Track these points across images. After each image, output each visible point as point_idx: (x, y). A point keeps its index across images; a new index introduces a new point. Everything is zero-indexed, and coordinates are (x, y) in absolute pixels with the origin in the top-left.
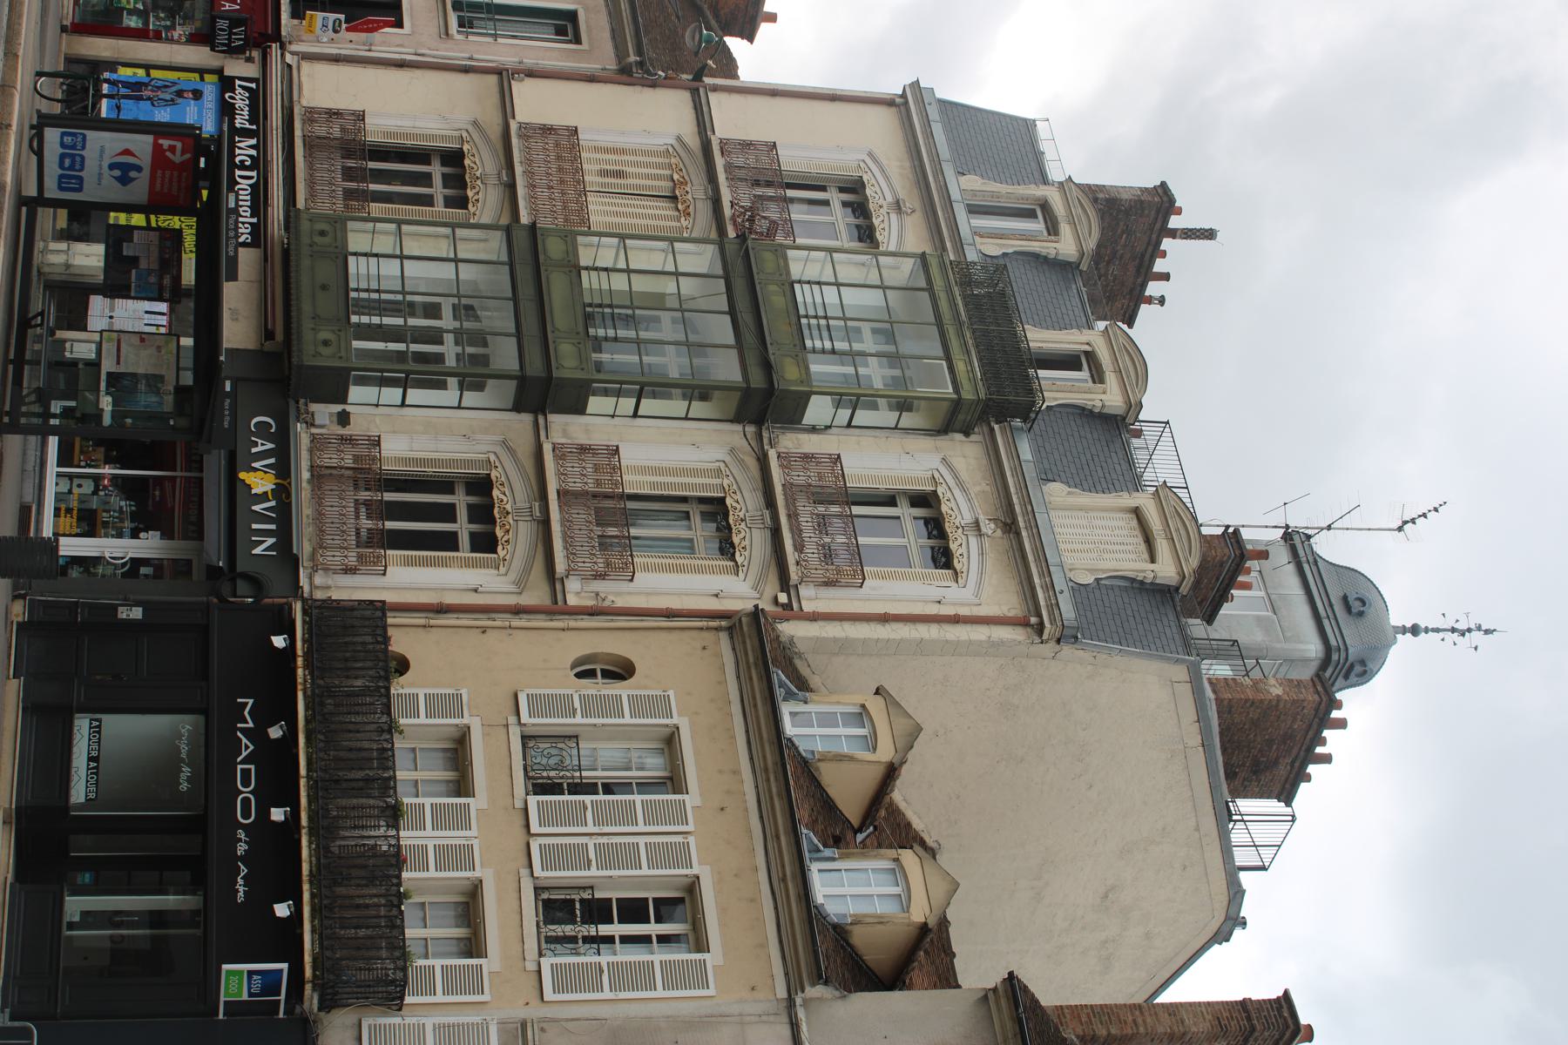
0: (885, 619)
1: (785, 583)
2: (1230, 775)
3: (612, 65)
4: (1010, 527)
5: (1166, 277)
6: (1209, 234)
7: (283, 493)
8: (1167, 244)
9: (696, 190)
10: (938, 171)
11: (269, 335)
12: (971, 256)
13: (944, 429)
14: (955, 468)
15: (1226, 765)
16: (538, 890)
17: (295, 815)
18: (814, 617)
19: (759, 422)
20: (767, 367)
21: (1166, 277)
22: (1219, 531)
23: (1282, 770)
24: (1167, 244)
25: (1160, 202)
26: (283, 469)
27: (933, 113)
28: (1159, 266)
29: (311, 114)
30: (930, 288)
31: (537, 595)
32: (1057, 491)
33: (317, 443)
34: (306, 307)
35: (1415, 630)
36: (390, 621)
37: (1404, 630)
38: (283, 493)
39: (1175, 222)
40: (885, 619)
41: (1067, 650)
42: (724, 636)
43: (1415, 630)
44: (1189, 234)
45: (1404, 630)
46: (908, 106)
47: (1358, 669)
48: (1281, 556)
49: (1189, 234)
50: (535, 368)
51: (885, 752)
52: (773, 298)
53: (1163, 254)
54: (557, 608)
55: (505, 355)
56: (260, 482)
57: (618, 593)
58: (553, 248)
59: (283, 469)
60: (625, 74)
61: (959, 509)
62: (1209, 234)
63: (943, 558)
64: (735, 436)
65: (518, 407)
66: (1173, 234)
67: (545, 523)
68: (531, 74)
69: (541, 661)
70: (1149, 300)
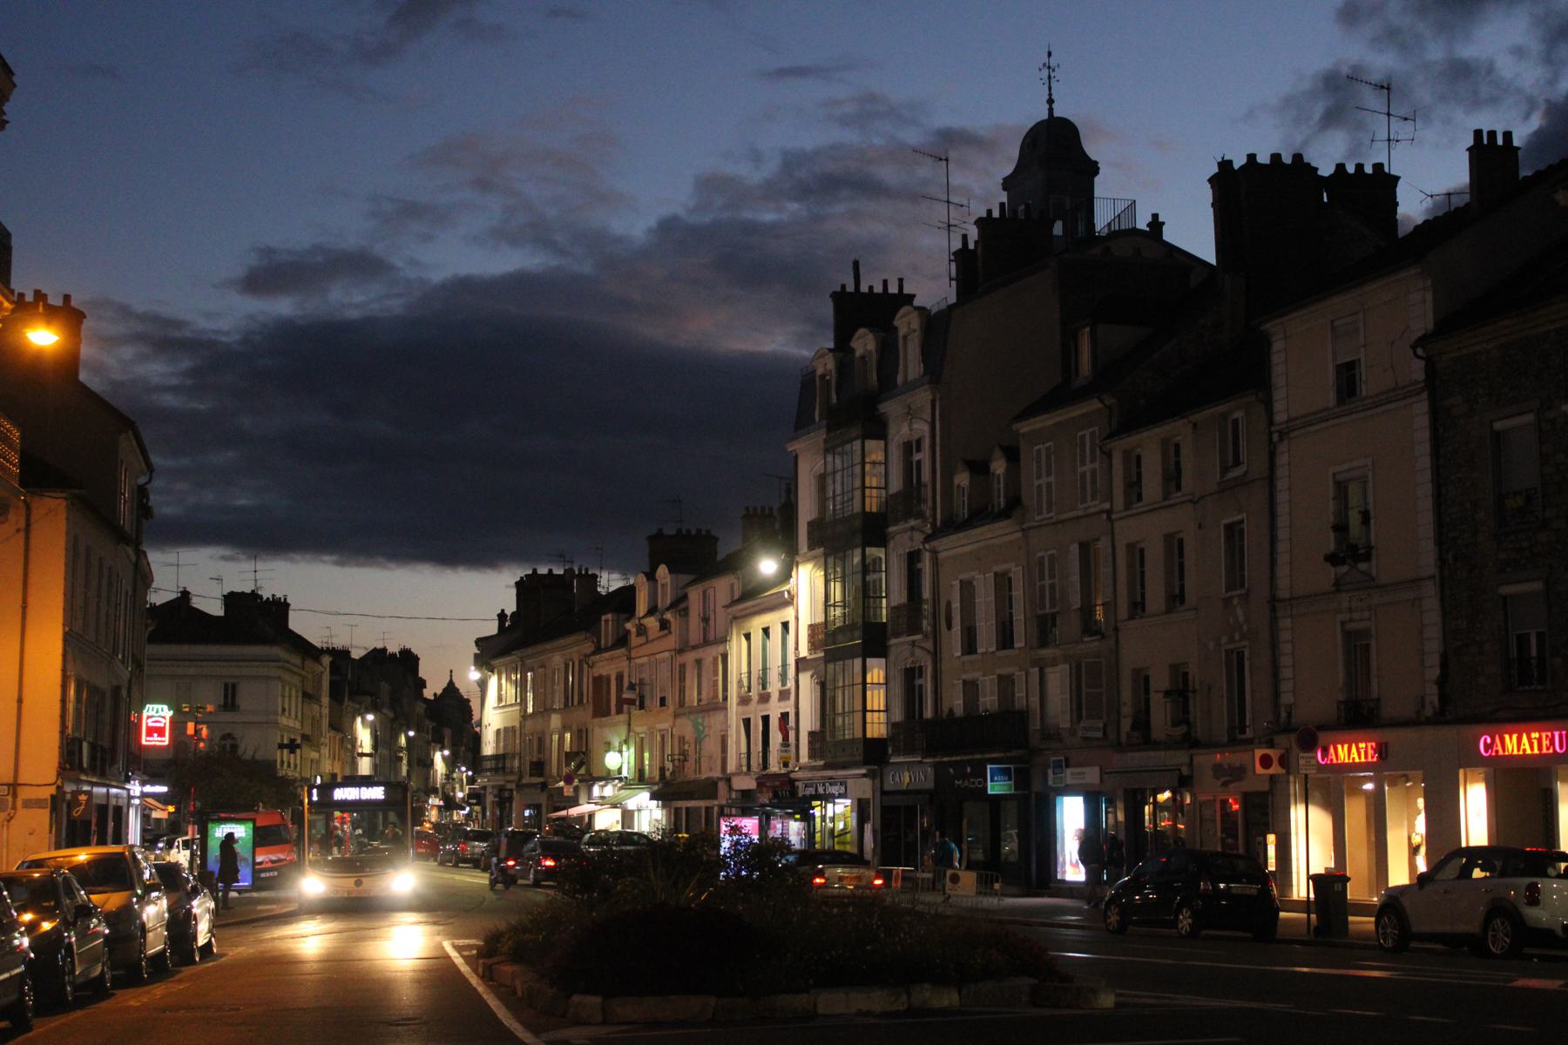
5: (885, 283)
6: (856, 265)
8: (864, 288)
17: (970, 762)
21: (885, 283)
22: (953, 266)
25: (840, 298)
28: (878, 289)
33: (897, 752)
35: (1050, 101)
37: (1051, 110)
39: (850, 288)
43: (1050, 101)
45: (1051, 110)
53: (871, 288)
62: (856, 265)
68: (797, 649)
70: (901, 287)
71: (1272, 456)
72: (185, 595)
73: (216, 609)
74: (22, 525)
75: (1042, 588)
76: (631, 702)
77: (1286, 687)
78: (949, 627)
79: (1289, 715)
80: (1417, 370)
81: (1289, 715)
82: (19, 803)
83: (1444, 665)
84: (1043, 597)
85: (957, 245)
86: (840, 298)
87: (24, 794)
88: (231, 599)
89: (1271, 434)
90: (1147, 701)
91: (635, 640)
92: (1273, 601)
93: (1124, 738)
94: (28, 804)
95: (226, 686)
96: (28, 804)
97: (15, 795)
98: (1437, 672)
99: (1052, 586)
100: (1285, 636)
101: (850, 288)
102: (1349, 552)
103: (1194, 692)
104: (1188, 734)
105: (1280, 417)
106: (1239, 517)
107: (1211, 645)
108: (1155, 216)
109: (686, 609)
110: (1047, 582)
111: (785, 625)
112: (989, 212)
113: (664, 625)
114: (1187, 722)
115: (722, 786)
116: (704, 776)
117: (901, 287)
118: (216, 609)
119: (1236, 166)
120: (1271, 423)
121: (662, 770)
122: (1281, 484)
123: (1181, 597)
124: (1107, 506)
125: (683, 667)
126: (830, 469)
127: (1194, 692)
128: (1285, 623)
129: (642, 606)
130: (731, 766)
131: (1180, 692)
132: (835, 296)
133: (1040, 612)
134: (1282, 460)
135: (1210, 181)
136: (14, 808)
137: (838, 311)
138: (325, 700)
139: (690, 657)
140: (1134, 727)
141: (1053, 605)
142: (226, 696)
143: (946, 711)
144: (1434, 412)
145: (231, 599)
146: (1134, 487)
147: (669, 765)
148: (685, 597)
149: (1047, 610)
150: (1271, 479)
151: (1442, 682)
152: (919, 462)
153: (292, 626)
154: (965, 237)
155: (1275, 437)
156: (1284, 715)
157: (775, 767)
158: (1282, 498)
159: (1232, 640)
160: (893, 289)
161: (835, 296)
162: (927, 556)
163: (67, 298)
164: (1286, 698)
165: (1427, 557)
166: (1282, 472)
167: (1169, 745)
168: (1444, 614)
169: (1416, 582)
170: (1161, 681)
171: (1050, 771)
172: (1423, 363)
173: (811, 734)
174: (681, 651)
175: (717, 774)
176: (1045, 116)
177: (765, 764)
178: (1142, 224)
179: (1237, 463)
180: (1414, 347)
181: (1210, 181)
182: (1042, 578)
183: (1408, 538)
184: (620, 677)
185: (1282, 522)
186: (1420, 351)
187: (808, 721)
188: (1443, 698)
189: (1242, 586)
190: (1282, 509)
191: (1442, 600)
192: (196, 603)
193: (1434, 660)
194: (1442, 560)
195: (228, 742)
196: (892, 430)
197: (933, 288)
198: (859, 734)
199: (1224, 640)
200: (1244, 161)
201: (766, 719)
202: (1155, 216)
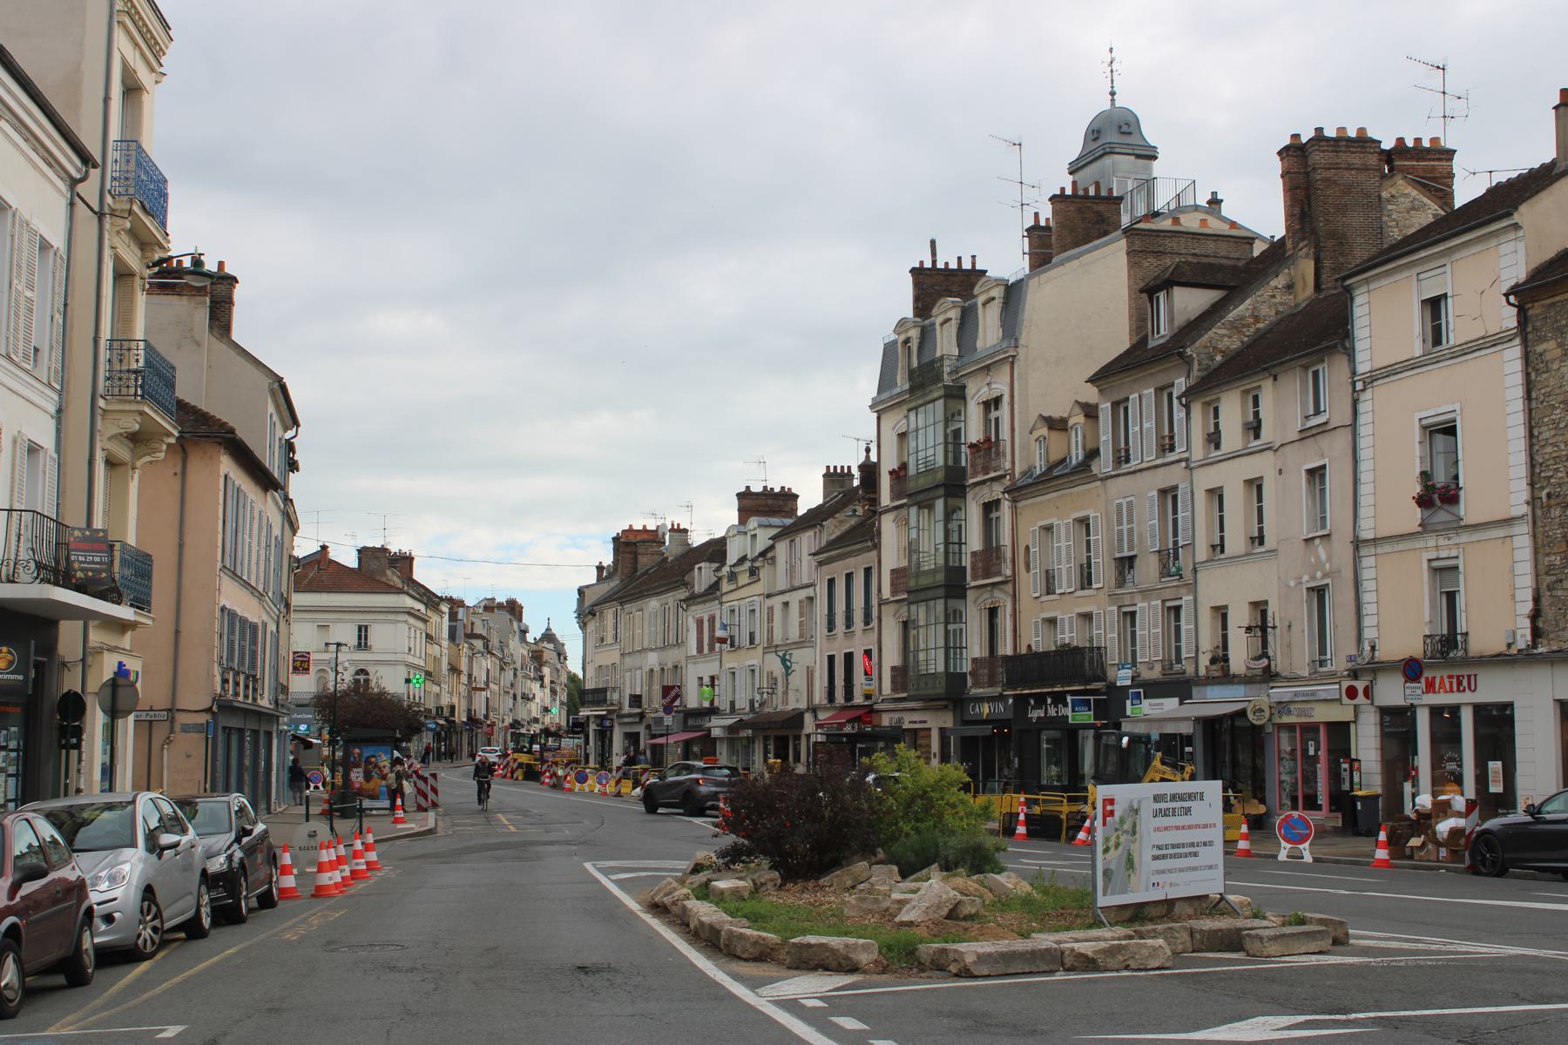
0: (1013, 430)
1: (1003, 477)
2: (1106, 233)
3: (875, 553)
4: (988, 368)
6: (933, 243)
7: (990, 699)
8: (940, 265)
9: (904, 512)
10: (892, 398)
11: (946, 707)
12: (907, 386)
13: (963, 398)
14: (978, 391)
15: (1099, 237)
16: (1083, 588)
18: (1013, 463)
19: (964, 487)
20: (937, 487)
23: (1101, 208)
24: (940, 265)
25: (918, 273)
26: (980, 700)
27: (885, 396)
28: (953, 265)
29: (894, 689)
30: (916, 408)
31: (1009, 588)
32: (979, 344)
33: (976, 684)
34: (931, 692)
35: (1113, 94)
36: (1009, 652)
37: (1113, 100)
38: (990, 699)
39: (928, 265)
40: (1013, 430)
41: (1021, 342)
42: (1020, 505)
43: (1113, 94)
44: (934, 254)
45: (1113, 100)
46: (881, 408)
47: (1125, 128)
48: (1079, 176)
49: (934, 254)
50: (941, 592)
51: (1044, 431)
52: (923, 483)
54: (1013, 580)
55: (940, 605)
56: (986, 709)
57: (1009, 555)
58: (912, 583)
59: (980, 700)
60: (877, 546)
61: (986, 394)
62: (933, 243)
63: (997, 401)
64: (970, 496)
65: (965, 597)
66: (934, 262)
67: (994, 585)
68: (880, 590)
69: (1030, 584)
70: (974, 264)
71: (1355, 402)
72: (324, 548)
73: (351, 561)
74: (178, 469)
75: (1120, 532)
76: (722, 641)
77: (1367, 622)
78: (1028, 570)
79: (1373, 648)
80: (1508, 318)
81: (1373, 648)
82: (177, 728)
83: (1537, 600)
84: (1120, 540)
85: (1030, 222)
86: (918, 273)
87: (182, 719)
88: (363, 552)
89: (1354, 383)
90: (1225, 638)
91: (725, 587)
92: (1357, 543)
93: (1202, 672)
94: (186, 728)
95: (360, 628)
96: (186, 728)
97: (172, 721)
98: (1529, 606)
99: (1131, 531)
100: (1367, 574)
101: (928, 265)
102: (1438, 496)
103: (1274, 627)
104: (1267, 669)
105: (1362, 368)
106: (1321, 463)
107: (1292, 583)
108: (1214, 194)
109: (773, 558)
110: (1125, 527)
111: (868, 571)
112: (1063, 189)
113: (753, 572)
114: (1265, 655)
115: (808, 718)
116: (790, 708)
117: (974, 264)
118: (351, 561)
119: (1304, 140)
120: (1354, 373)
121: (752, 702)
122: (1364, 430)
123: (1260, 539)
124: (1186, 455)
125: (771, 609)
126: (913, 426)
127: (1274, 627)
128: (1367, 562)
129: (732, 556)
130: (817, 701)
131: (1261, 626)
132: (913, 271)
133: (1118, 555)
134: (1361, 408)
135: (1279, 153)
136: (172, 731)
137: (917, 285)
138: (445, 643)
139: (777, 602)
140: (1213, 661)
141: (1131, 548)
142: (360, 637)
143: (1024, 651)
144: (1527, 358)
145: (363, 552)
146: (1214, 439)
147: (758, 697)
148: (772, 547)
149: (1126, 553)
150: (1354, 426)
151: (1535, 616)
152: (997, 419)
153: (415, 577)
154: (1036, 215)
155: (1359, 386)
156: (1367, 648)
157: (858, 699)
158: (1364, 443)
159: (1313, 578)
160: (967, 265)
161: (913, 271)
162: (1006, 506)
163: (221, 264)
164: (1369, 634)
165: (1517, 499)
166: (1362, 419)
167: (1247, 680)
168: (1536, 552)
169: (1508, 521)
170: (1240, 617)
171: (1128, 702)
172: (1515, 310)
173: (893, 669)
174: (769, 596)
175: (803, 705)
176: (1107, 106)
177: (849, 694)
178: (1202, 200)
179: (1317, 412)
180: (1507, 295)
181: (1279, 153)
182: (1120, 523)
183: (1496, 476)
184: (712, 619)
185: (1365, 466)
186: (1512, 299)
187: (891, 656)
188: (1536, 633)
189: (1323, 526)
190: (1365, 454)
191: (1534, 536)
192: (334, 555)
193: (1528, 595)
194: (1533, 501)
195: (362, 678)
196: (970, 391)
197: (1005, 258)
198: (941, 668)
199: (1306, 578)
200: (1312, 134)
201: (849, 657)
202: (1214, 194)
